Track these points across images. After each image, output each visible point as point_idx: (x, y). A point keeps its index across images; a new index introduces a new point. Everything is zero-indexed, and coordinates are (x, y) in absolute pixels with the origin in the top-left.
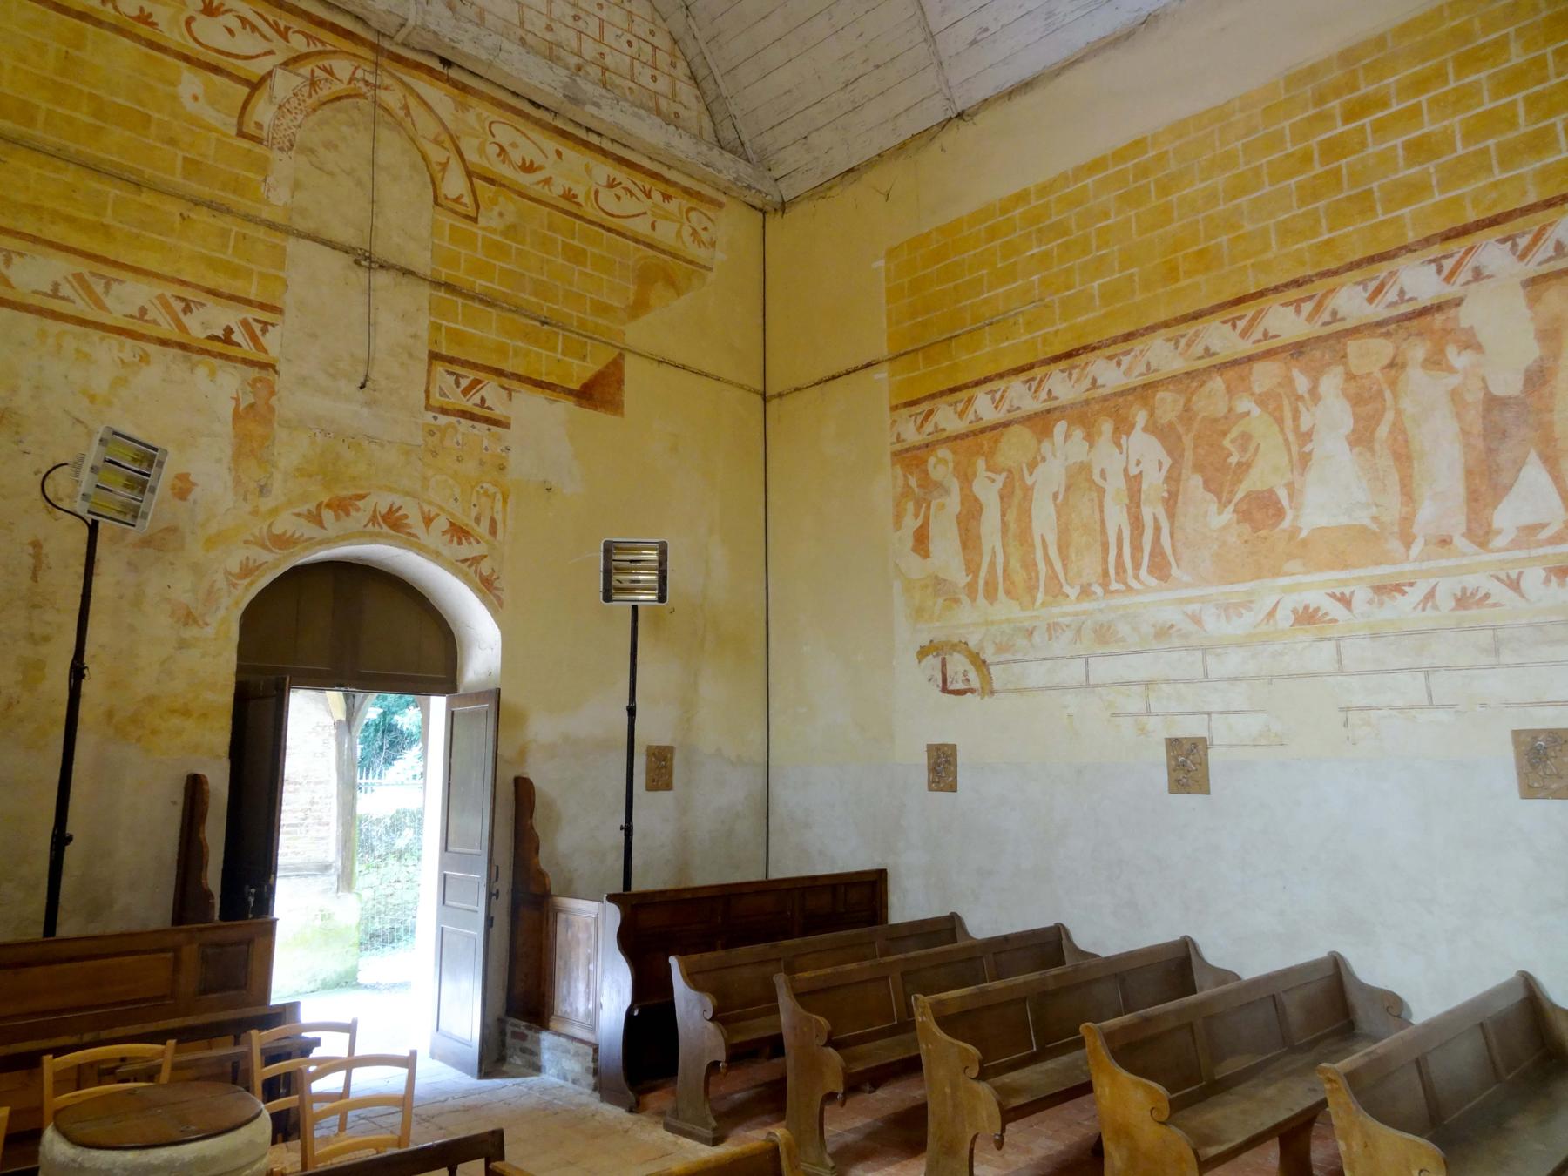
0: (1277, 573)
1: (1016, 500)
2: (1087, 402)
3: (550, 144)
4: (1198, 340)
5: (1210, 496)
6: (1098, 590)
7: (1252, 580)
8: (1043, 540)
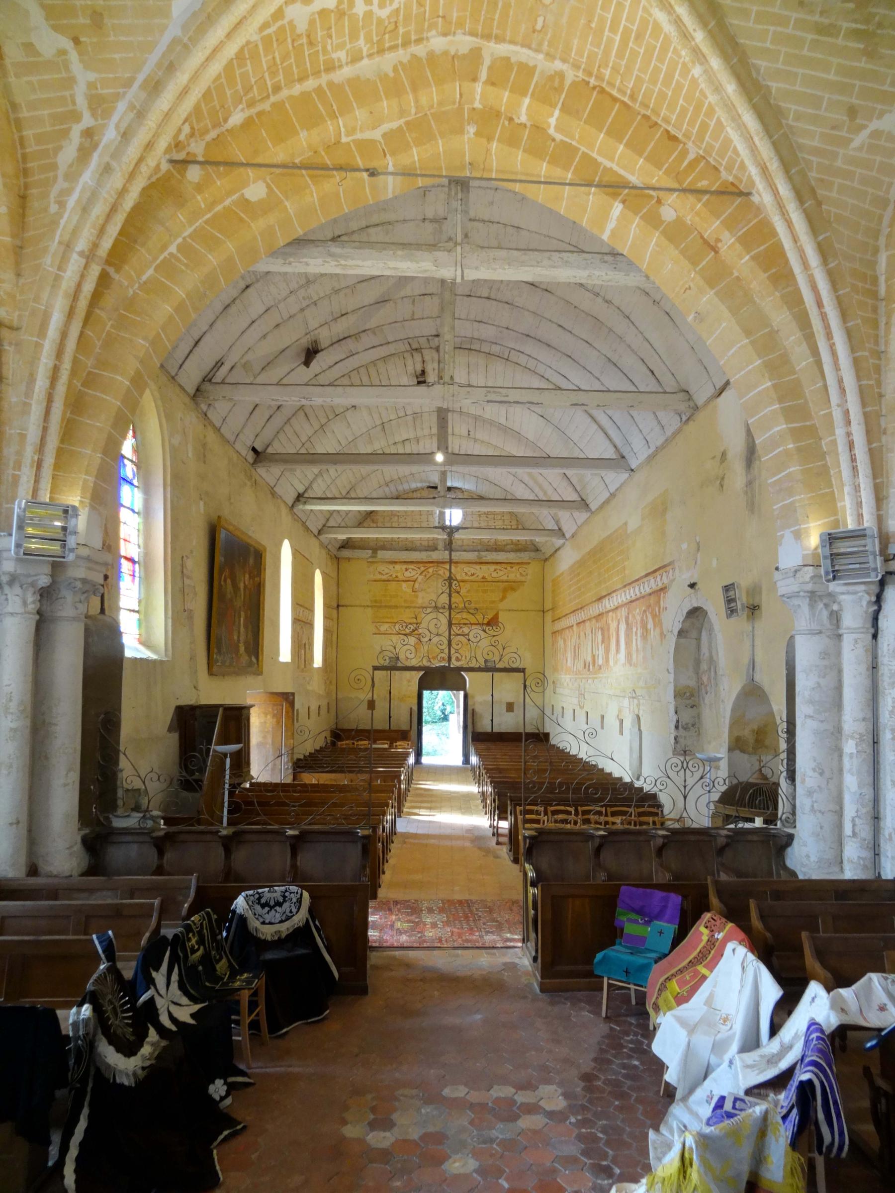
3: (478, 567)
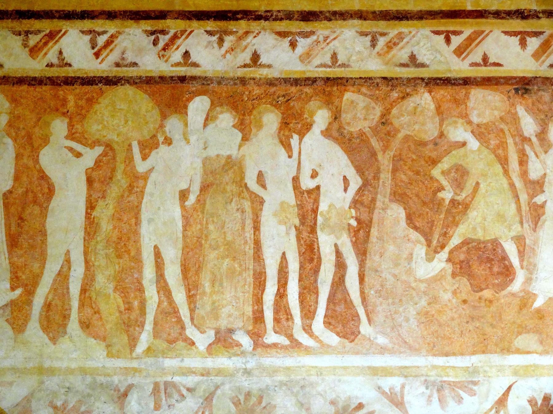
0: (507, 350)
1: (114, 191)
2: (243, 81)
4: (401, 44)
5: (414, 235)
6: (246, 341)
7: (474, 353)
8: (158, 254)
